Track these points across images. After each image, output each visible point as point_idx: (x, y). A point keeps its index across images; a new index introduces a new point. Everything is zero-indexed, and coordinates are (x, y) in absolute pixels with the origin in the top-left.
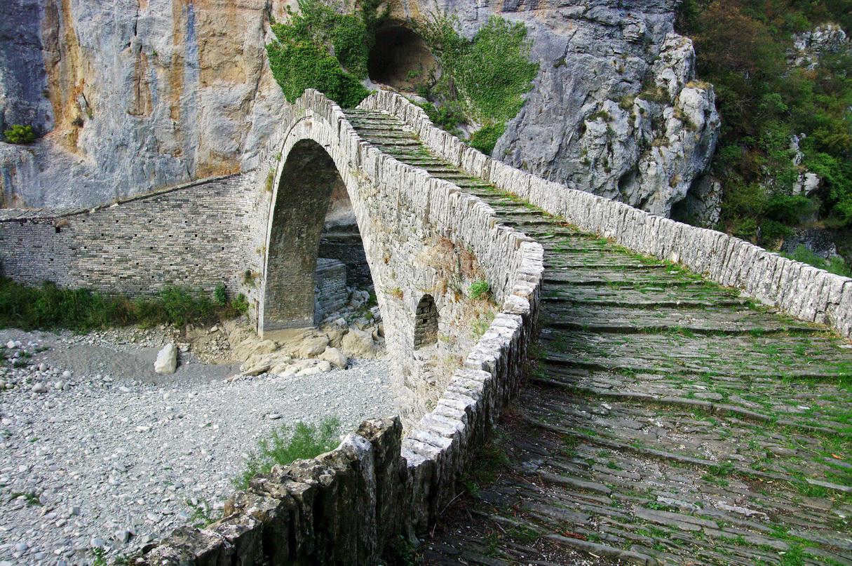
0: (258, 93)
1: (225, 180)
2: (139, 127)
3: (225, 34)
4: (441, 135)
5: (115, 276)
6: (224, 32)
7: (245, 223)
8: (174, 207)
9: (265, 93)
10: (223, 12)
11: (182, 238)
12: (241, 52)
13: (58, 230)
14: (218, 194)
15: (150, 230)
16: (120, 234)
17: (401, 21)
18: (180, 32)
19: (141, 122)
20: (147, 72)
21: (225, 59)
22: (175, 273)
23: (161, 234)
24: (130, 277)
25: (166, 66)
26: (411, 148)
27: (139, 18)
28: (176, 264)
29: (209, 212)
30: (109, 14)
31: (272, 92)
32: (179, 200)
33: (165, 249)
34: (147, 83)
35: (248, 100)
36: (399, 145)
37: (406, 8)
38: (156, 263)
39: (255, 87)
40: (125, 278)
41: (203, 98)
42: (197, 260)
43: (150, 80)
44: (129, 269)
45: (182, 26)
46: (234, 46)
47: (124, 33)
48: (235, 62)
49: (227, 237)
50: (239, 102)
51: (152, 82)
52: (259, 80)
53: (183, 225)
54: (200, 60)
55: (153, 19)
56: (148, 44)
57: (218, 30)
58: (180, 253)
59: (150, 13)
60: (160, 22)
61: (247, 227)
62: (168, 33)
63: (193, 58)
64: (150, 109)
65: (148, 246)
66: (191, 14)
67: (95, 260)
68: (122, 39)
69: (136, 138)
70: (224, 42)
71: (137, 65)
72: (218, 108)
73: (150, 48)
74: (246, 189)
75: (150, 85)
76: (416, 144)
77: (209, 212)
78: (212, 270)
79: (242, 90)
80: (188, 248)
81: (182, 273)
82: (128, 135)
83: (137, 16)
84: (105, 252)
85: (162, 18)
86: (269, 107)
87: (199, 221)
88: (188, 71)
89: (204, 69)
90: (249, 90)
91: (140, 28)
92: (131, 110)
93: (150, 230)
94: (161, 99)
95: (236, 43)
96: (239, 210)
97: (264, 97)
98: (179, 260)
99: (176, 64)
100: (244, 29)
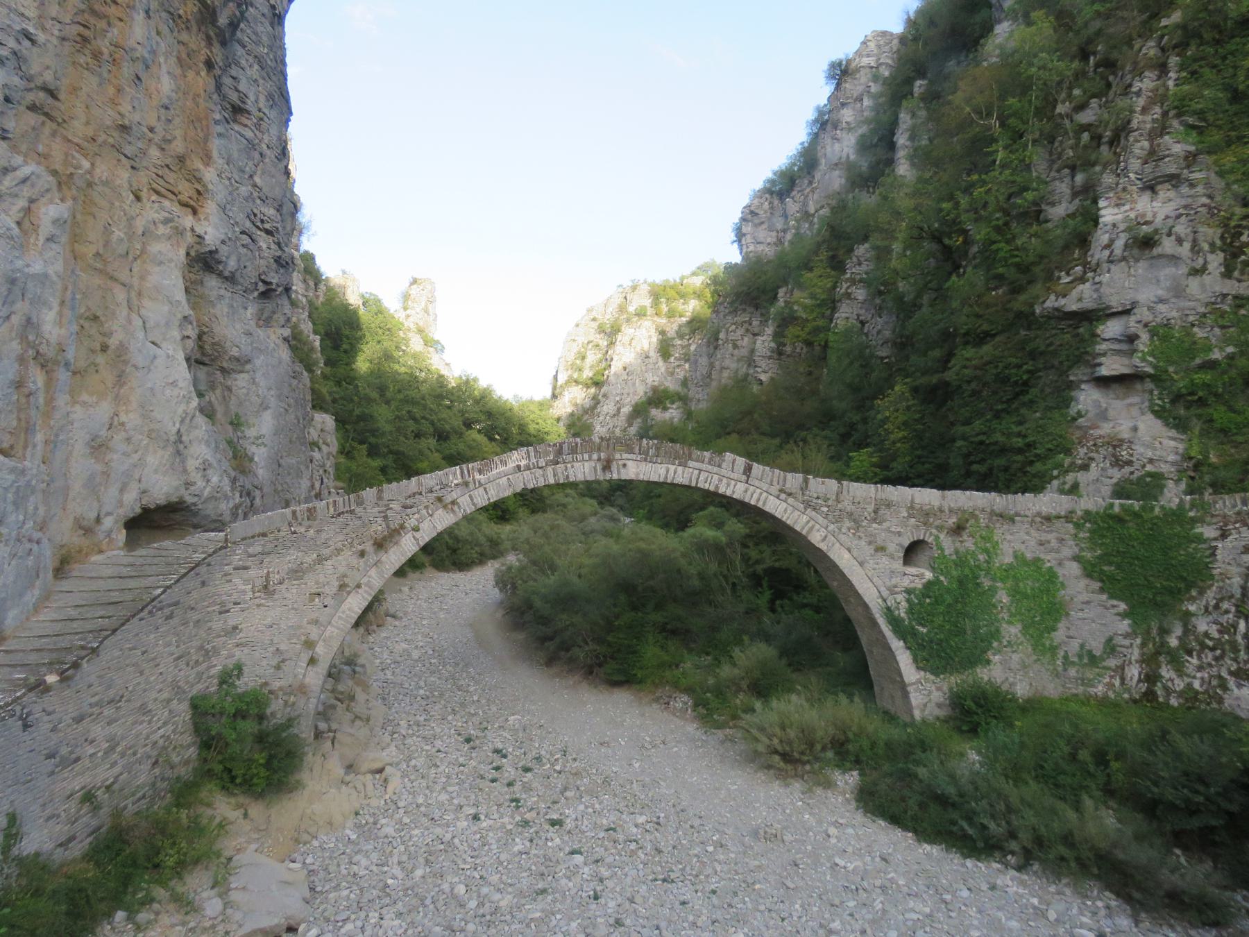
7: (231, 623)
9: (123, 418)
12: (104, 348)
13: (26, 726)
14: (203, 584)
24: (116, 778)
33: (156, 700)
41: (76, 425)
49: (207, 652)
53: (173, 648)
67: (78, 767)
79: (104, 410)
81: (168, 737)
96: (222, 604)
97: (122, 424)
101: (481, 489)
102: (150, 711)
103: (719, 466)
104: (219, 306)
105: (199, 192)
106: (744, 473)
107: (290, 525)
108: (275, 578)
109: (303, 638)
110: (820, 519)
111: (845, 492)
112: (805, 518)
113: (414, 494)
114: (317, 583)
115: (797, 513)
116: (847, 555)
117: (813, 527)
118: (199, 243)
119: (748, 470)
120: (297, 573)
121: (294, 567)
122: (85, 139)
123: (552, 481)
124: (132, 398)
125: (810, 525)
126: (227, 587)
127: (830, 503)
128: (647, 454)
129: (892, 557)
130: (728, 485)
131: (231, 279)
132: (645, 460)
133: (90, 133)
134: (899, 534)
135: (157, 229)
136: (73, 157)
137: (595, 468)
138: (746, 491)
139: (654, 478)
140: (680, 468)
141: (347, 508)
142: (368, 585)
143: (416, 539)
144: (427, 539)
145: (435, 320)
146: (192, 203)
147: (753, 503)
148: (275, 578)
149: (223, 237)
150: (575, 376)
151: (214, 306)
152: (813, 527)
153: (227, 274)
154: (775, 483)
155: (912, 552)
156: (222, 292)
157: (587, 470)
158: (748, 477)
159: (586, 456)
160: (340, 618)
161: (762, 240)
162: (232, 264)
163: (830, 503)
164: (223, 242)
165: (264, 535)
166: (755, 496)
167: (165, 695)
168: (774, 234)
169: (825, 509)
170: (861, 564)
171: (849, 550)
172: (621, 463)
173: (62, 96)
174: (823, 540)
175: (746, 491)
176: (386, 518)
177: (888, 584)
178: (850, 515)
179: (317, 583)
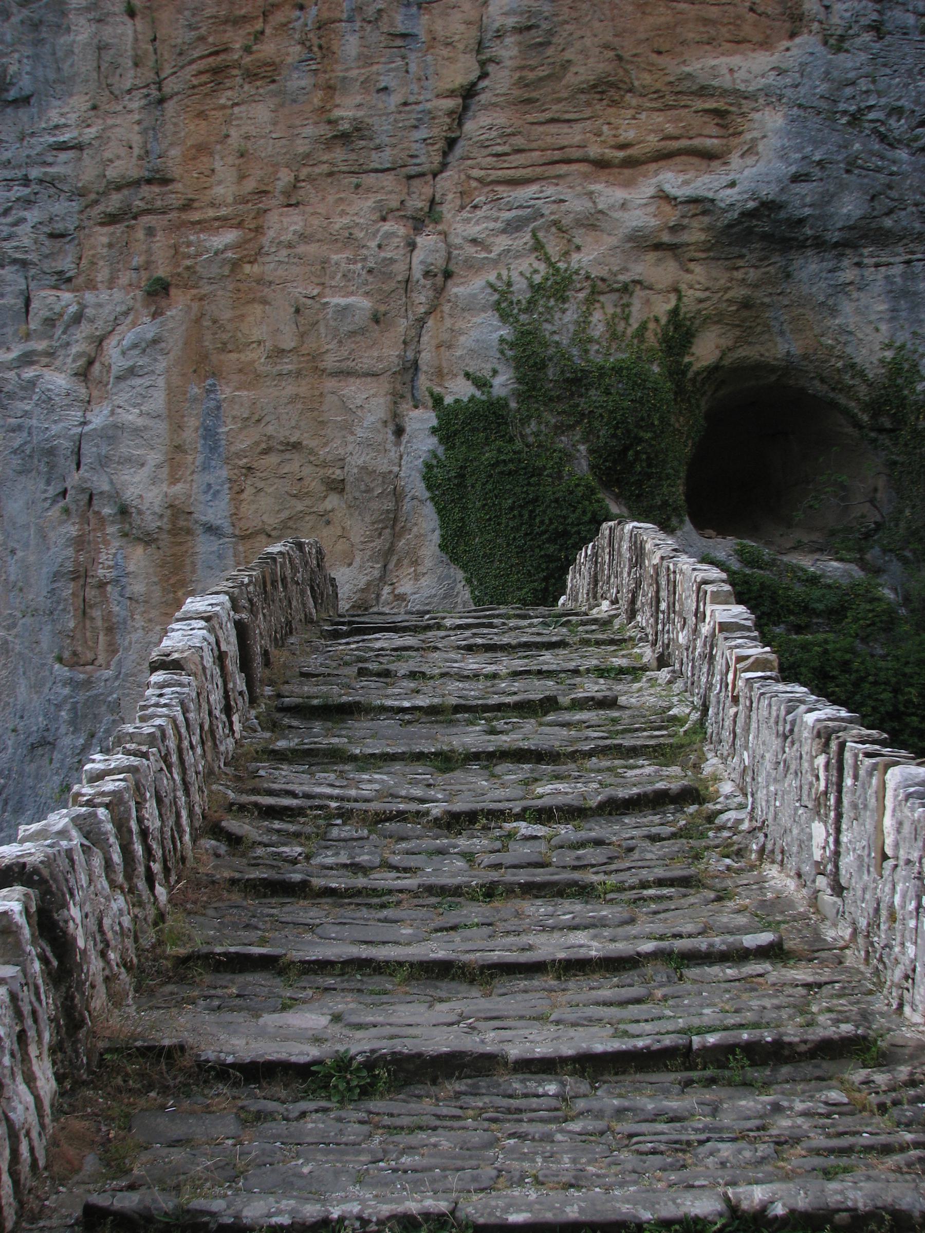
0: (387, 589)
2: (82, 696)
3: (296, 446)
4: (809, 745)
6: (293, 439)
9: (405, 587)
10: (290, 389)
17: (773, 369)
18: (185, 452)
19: (88, 683)
20: (103, 557)
21: (300, 506)
25: (148, 540)
26: (627, 829)
27: (87, 428)
30: (20, 428)
31: (424, 581)
34: (102, 585)
36: (544, 815)
37: (782, 333)
39: (376, 573)
43: (111, 574)
45: (190, 435)
46: (322, 472)
47: (52, 466)
48: (327, 512)
51: (116, 581)
52: (391, 551)
54: (235, 516)
55: (118, 427)
56: (106, 487)
57: (282, 433)
59: (112, 413)
60: (137, 431)
62: (154, 457)
63: (216, 512)
64: (112, 649)
66: (212, 404)
68: (48, 483)
69: (75, 723)
70: (294, 464)
71: (79, 543)
73: (115, 496)
75: (109, 588)
76: (657, 801)
82: (56, 718)
83: (84, 424)
85: (140, 422)
88: (204, 546)
89: (243, 538)
90: (362, 581)
91: (89, 452)
92: (66, 655)
94: (139, 621)
95: (325, 465)
99: (175, 531)
100: (347, 427)
104: (847, 307)
105: (716, 112)
118: (704, 213)
122: (242, 200)
131: (865, 236)
133: (250, 185)
135: (487, 248)
136: (189, 244)
149: (793, 169)
151: (834, 312)
153: (836, 236)
156: (849, 275)
162: (849, 207)
164: (796, 178)
173: (176, 171)
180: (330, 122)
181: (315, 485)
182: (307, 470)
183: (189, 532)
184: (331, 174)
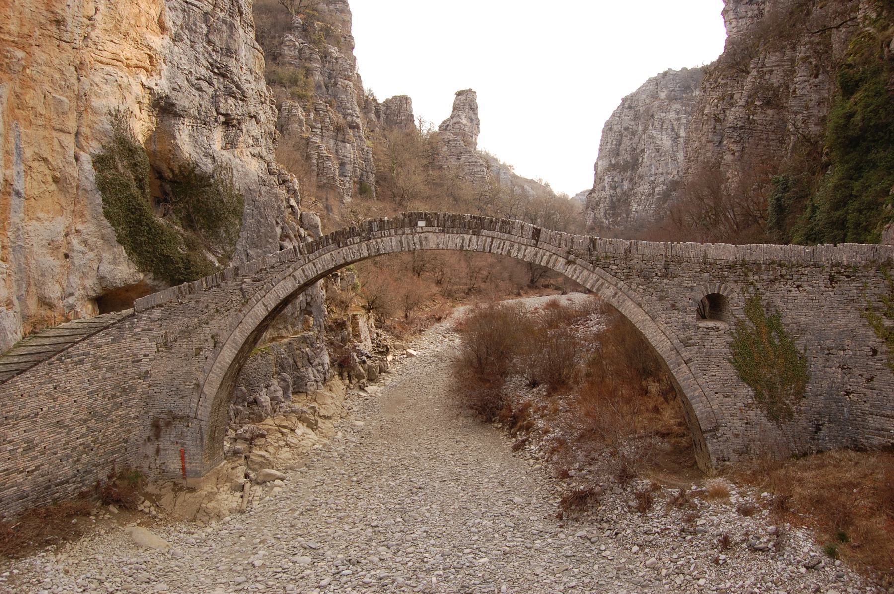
1: (119, 324)
5: (22, 472)
7: (144, 369)
8: (77, 364)
10: (42, 133)
11: (87, 401)
15: (55, 399)
16: (26, 412)
22: (82, 447)
23: (66, 402)
28: (83, 436)
29: (107, 363)
32: (79, 355)
33: (72, 419)
35: (66, 235)
38: (63, 441)
40: (33, 471)
42: (100, 425)
44: (36, 457)
49: (124, 390)
50: (61, 238)
58: (86, 421)
61: (147, 372)
65: (55, 420)
72: (43, 246)
74: (143, 330)
77: (107, 363)
78: (114, 432)
80: (93, 413)
81: (88, 446)
84: (10, 442)
86: (85, 242)
87: (100, 377)
93: (55, 399)
95: (54, 170)
96: (135, 355)
97: (77, 231)
98: (84, 430)
101: (311, 264)
102: (67, 426)
103: (509, 233)
106: (533, 238)
107: (178, 297)
108: (171, 338)
109: (194, 381)
110: (609, 277)
111: (633, 251)
112: (594, 277)
113: (261, 270)
114: (199, 340)
115: (585, 273)
116: (637, 309)
117: (603, 284)
119: (537, 233)
120: (187, 333)
121: (183, 328)
123: (366, 254)
124: (85, 212)
125: (599, 283)
126: (137, 344)
127: (618, 261)
128: (444, 227)
129: (685, 310)
130: (519, 249)
132: (443, 231)
134: (692, 288)
137: (401, 241)
138: (536, 254)
139: (451, 245)
140: (474, 238)
141: (215, 283)
142: (235, 341)
143: (265, 306)
144: (273, 306)
145: (478, 124)
146: (140, 64)
147: (543, 264)
148: (171, 338)
150: (613, 162)
152: (603, 284)
154: (563, 245)
155: (713, 306)
157: (394, 244)
158: (537, 241)
159: (393, 231)
160: (217, 367)
161: (744, 14)
163: (618, 261)
165: (161, 306)
166: (545, 258)
167: (82, 416)
168: (755, 7)
169: (614, 267)
170: (653, 318)
171: (640, 305)
172: (422, 235)
174: (614, 297)
175: (536, 254)
176: (241, 289)
177: (682, 337)
178: (640, 273)
179: (199, 340)
180: (52, 13)
181: (50, 179)
182: (47, 172)
183: (10, 194)
184: (50, 37)
